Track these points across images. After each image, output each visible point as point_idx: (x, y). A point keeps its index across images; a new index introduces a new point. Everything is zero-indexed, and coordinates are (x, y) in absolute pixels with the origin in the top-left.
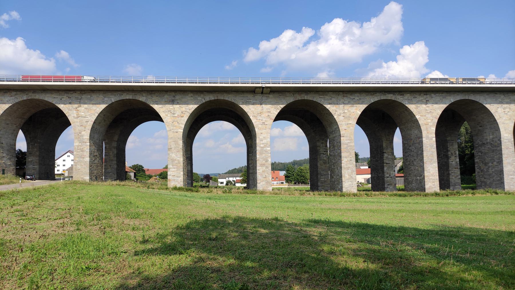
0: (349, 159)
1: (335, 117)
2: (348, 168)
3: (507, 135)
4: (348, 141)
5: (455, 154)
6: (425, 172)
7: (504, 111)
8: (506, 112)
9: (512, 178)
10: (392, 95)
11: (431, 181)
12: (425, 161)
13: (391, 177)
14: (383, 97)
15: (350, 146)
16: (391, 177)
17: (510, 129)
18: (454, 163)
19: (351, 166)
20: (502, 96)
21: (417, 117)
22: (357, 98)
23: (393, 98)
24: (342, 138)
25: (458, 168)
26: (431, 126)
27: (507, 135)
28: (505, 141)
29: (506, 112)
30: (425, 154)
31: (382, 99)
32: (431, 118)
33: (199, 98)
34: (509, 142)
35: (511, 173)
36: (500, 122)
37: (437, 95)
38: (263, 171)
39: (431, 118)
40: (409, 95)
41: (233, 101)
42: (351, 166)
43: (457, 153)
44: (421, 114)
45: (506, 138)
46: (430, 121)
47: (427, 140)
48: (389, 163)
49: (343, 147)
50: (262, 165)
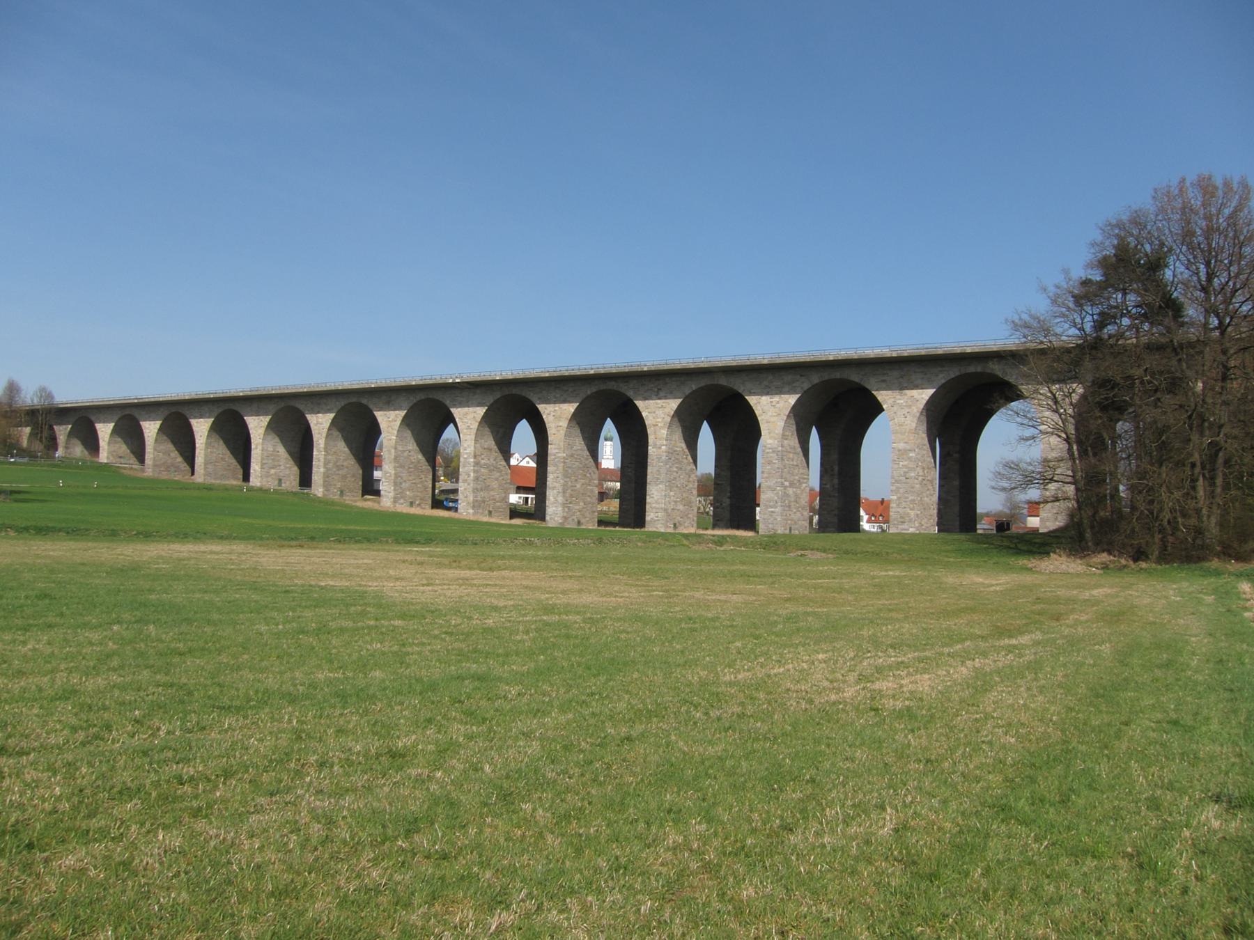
0: (555, 475)
1: (544, 417)
2: (554, 488)
3: (770, 441)
4: (557, 451)
5: (832, 470)
6: (648, 497)
7: (771, 402)
8: (774, 404)
9: (772, 512)
10: (613, 383)
11: (654, 510)
12: (648, 481)
13: (723, 508)
14: (603, 387)
15: (559, 457)
16: (723, 508)
17: (777, 432)
18: (828, 486)
19: (557, 485)
20: (771, 377)
21: (644, 414)
22: (571, 390)
23: (615, 388)
24: (549, 446)
25: (834, 496)
26: (662, 428)
27: (770, 441)
28: (768, 451)
29: (774, 404)
30: (650, 470)
31: (602, 388)
32: (663, 416)
33: (411, 398)
34: (773, 452)
35: (771, 504)
36: (762, 420)
37: (674, 379)
38: (465, 489)
39: (663, 416)
40: (635, 381)
41: (441, 400)
42: (557, 485)
43: (836, 468)
44: (649, 410)
45: (769, 446)
46: (660, 420)
47: (654, 450)
48: (722, 484)
49: (550, 458)
50: (465, 481)
